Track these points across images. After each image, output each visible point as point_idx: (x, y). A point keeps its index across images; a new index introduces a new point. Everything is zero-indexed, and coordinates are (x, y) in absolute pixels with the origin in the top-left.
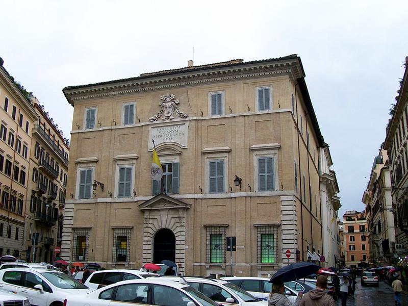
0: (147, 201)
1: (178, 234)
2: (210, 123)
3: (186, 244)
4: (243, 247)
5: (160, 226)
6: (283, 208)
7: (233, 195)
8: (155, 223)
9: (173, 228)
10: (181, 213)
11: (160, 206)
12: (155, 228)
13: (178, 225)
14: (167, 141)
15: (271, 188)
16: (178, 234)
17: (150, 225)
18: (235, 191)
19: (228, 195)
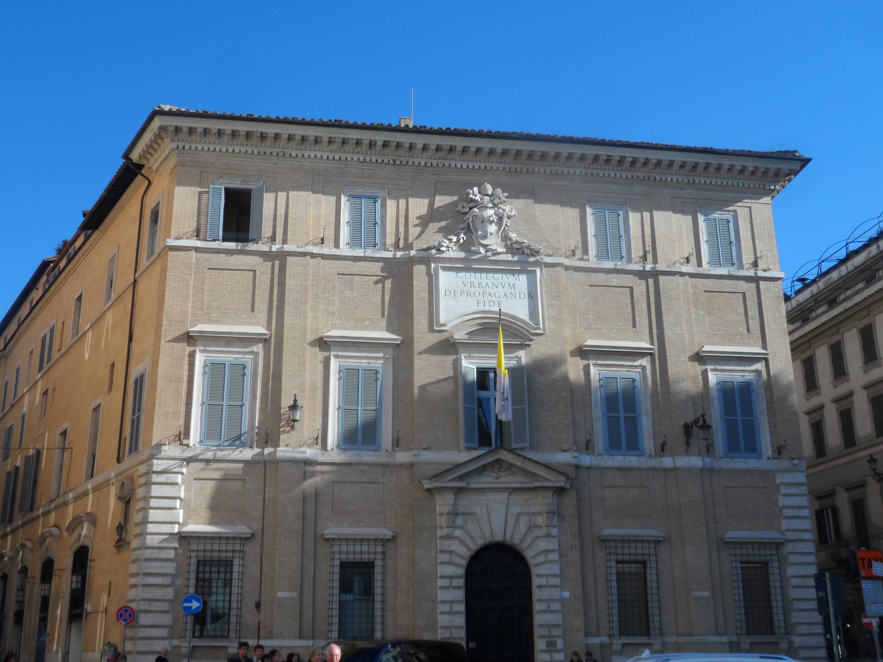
1: (541, 558)
2: (601, 278)
3: (562, 587)
4: (707, 594)
5: (488, 533)
7: (667, 462)
8: (471, 527)
9: (528, 542)
11: (483, 479)
12: (472, 538)
13: (540, 532)
14: (487, 308)
15: (752, 448)
16: (541, 558)
17: (457, 533)
18: (673, 454)
19: (653, 463)
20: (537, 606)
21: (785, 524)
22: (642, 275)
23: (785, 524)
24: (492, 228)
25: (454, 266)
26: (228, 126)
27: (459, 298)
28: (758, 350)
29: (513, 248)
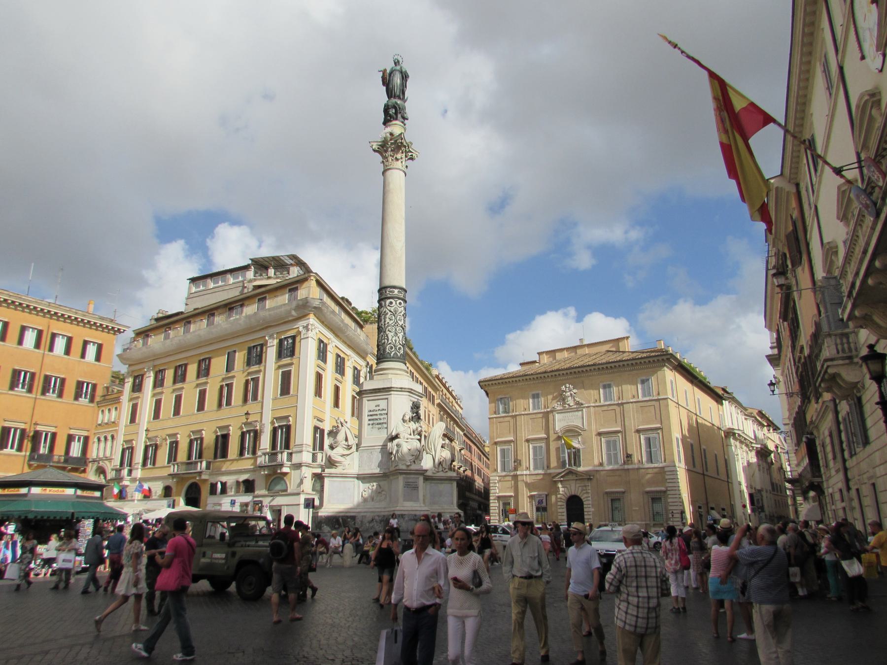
0: (560, 473)
2: (605, 408)
6: (667, 477)
7: (626, 467)
20: (565, 514)
21: (668, 485)
22: (618, 405)
24: (570, 398)
25: (560, 412)
26: (497, 382)
27: (560, 422)
28: (659, 425)
29: (578, 403)
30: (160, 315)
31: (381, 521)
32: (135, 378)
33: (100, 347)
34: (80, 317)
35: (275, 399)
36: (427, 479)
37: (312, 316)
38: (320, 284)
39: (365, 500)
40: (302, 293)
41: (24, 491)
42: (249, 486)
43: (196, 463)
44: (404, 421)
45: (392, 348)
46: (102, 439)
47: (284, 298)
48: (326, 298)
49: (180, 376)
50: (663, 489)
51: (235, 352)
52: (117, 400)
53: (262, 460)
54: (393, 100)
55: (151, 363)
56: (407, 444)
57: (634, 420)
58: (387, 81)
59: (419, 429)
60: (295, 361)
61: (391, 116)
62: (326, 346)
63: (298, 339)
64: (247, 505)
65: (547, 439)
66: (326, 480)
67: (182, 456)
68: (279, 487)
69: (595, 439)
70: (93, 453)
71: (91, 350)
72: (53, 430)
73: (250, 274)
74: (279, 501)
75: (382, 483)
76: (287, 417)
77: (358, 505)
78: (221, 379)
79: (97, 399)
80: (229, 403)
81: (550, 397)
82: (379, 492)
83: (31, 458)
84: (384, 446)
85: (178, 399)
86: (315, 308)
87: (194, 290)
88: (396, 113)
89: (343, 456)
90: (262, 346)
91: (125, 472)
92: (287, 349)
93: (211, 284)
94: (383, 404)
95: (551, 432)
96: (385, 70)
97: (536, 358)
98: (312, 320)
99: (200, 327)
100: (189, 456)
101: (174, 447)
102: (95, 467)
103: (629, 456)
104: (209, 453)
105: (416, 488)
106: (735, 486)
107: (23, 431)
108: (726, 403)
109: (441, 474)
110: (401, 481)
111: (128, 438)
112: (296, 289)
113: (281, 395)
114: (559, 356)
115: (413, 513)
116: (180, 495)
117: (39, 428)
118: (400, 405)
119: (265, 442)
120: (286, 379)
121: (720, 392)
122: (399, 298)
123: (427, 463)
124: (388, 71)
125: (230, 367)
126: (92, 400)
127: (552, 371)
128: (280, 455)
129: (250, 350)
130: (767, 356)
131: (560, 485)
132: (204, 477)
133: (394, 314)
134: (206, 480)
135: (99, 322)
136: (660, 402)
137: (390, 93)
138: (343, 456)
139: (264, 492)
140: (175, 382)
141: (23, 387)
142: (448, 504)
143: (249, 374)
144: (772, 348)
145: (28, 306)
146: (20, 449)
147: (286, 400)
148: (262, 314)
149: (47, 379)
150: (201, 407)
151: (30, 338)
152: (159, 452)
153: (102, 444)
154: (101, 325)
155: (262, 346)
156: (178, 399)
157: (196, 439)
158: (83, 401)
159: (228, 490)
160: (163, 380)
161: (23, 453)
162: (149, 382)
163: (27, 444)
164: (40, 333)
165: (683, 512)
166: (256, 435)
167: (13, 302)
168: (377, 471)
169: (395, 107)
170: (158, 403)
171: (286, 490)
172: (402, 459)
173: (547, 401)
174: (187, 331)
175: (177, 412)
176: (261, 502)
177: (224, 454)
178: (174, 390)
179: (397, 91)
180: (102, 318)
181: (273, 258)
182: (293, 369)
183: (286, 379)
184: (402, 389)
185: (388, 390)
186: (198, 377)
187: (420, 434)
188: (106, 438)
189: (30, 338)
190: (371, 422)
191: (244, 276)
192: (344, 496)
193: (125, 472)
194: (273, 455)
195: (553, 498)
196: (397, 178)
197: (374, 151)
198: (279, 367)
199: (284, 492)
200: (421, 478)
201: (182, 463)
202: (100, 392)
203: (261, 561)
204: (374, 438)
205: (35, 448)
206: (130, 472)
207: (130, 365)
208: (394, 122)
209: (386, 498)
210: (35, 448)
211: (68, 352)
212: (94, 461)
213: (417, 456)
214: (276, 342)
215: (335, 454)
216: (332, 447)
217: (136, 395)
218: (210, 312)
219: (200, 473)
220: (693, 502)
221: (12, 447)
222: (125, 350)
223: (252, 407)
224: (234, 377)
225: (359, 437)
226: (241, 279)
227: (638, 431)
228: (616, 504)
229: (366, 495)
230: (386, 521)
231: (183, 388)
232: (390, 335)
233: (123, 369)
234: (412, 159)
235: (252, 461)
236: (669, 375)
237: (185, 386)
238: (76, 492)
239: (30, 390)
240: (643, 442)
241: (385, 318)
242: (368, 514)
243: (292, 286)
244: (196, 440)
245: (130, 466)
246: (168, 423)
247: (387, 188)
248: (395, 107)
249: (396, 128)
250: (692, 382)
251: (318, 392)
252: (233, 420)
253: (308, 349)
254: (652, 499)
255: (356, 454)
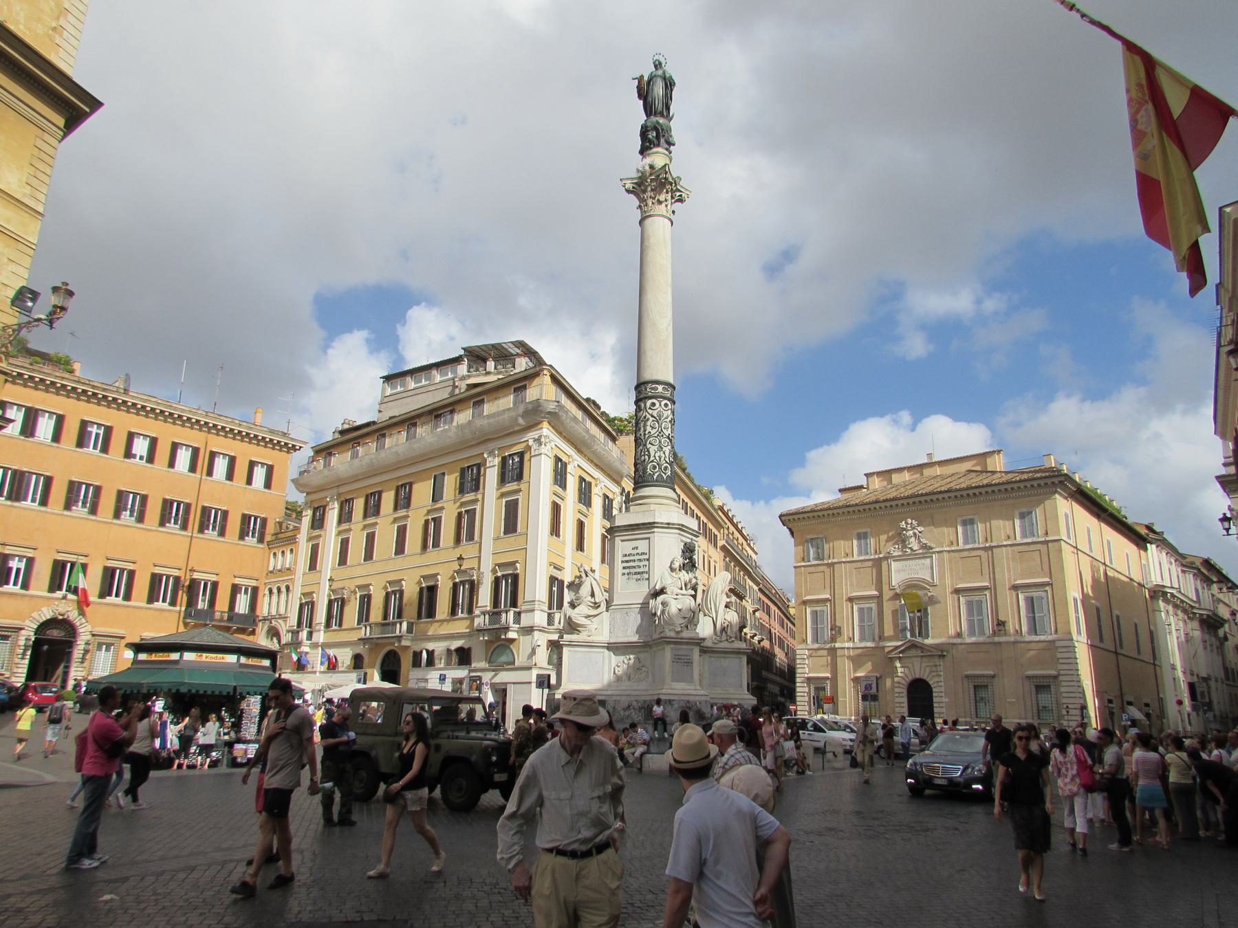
0: (897, 647)
2: (965, 554)
6: (1059, 656)
7: (997, 639)
10: (937, 661)
20: (906, 705)
21: (1061, 667)
22: (985, 549)
23: (1061, 667)
25: (897, 559)
27: (899, 573)
30: (346, 426)
31: (641, 708)
32: (315, 510)
33: (270, 470)
34: (245, 431)
35: (497, 539)
36: (705, 651)
37: (545, 424)
38: (557, 380)
39: (619, 679)
40: (532, 393)
41: (175, 656)
42: (463, 656)
43: (394, 624)
44: (672, 570)
45: (654, 467)
46: (275, 591)
47: (507, 401)
48: (565, 400)
49: (373, 508)
50: (1054, 672)
51: (443, 474)
52: (292, 540)
53: (479, 621)
54: (653, 119)
55: (335, 491)
56: (677, 602)
57: (1009, 571)
58: (644, 92)
59: (694, 581)
60: (523, 486)
61: (650, 142)
62: (565, 465)
63: (527, 457)
64: (461, 681)
65: (879, 598)
66: (565, 650)
67: (376, 615)
68: (503, 659)
69: (950, 600)
70: (263, 609)
71: (260, 474)
72: (214, 578)
73: (463, 369)
74: (503, 677)
75: (642, 656)
76: (513, 564)
77: (609, 685)
78: (425, 511)
79: (268, 538)
80: (436, 544)
81: (883, 537)
82: (637, 667)
83: (188, 615)
84: (645, 605)
85: (371, 538)
86: (549, 413)
87: (389, 391)
88: (658, 137)
89: (587, 617)
90: (479, 466)
91: (303, 635)
92: (514, 471)
93: (411, 384)
94: (642, 546)
95: (885, 588)
96: (642, 77)
97: (863, 481)
98: (546, 430)
99: (397, 442)
100: (386, 616)
101: (366, 601)
102: (266, 628)
103: (1001, 623)
104: (411, 611)
105: (689, 663)
106: (1166, 669)
107: (177, 579)
108: (1152, 548)
109: (725, 645)
110: (668, 653)
111: (307, 590)
112: (524, 387)
113: (505, 533)
114: (896, 478)
115: (686, 698)
116: (373, 667)
117: (196, 576)
118: (667, 548)
119: (484, 597)
120: (512, 511)
121: (1143, 531)
122: (665, 398)
123: (705, 629)
124: (646, 78)
125: (437, 496)
126: (261, 540)
127: (886, 500)
128: (504, 615)
129: (463, 472)
130: (1217, 478)
131: (898, 664)
132: (404, 643)
133: (658, 419)
134: (407, 647)
135: (268, 437)
136: (1049, 547)
137: (649, 110)
138: (587, 617)
139: (483, 664)
140: (365, 516)
141: (176, 523)
142: (737, 689)
143: (462, 504)
144: (1225, 465)
145: (180, 417)
146: (173, 603)
147: (512, 541)
148: (479, 423)
149: (206, 511)
150: (400, 549)
151: (184, 457)
152: (347, 609)
153: (275, 597)
154: (271, 440)
155: (479, 466)
156: (371, 538)
157: (394, 592)
158: (251, 540)
159: (437, 661)
160: (351, 512)
161: (178, 608)
162: (333, 515)
163: (183, 597)
164: (196, 452)
165: (1084, 707)
166: (473, 587)
167: (162, 412)
168: (635, 638)
169: (655, 128)
170: (345, 544)
171: (513, 663)
172: (669, 622)
173: (880, 544)
174: (381, 447)
175: (369, 556)
176: (480, 678)
177: (431, 613)
178: (365, 527)
179: (659, 106)
180: (272, 432)
181: (493, 345)
182: (520, 497)
183: (512, 511)
184: (669, 526)
185: (650, 526)
186: (396, 509)
187: (695, 588)
188: (279, 590)
189: (184, 457)
190: (627, 571)
191: (455, 372)
192: (591, 672)
193: (303, 635)
194: (495, 615)
195: (888, 682)
196: (659, 227)
197: (628, 191)
198: (503, 495)
199: (510, 665)
200: (696, 650)
201: (376, 624)
202: (270, 529)
203: (474, 758)
204: (631, 593)
205: (191, 602)
206: (310, 635)
207: (308, 494)
208: (655, 150)
209: (647, 676)
210: (191, 602)
211: (230, 476)
212: (265, 619)
213: (691, 619)
214: (497, 461)
215: (578, 615)
216: (573, 605)
217: (317, 532)
218: (409, 421)
219: (400, 638)
220: (1099, 693)
221: (164, 601)
222: (301, 473)
223: (467, 549)
224: (442, 508)
225: (610, 590)
226: (450, 376)
227: (1015, 588)
228: (982, 694)
229: (620, 671)
230: (647, 709)
231: (376, 524)
232: (652, 449)
233: (300, 498)
234: (681, 200)
235: (467, 623)
236: (1063, 506)
237: (378, 521)
238: (238, 659)
239: (184, 527)
240: (1022, 603)
241: (645, 426)
242: (623, 699)
243: (519, 384)
244: (394, 594)
245: (310, 626)
246: (358, 572)
247: (646, 243)
248: (655, 128)
249: (658, 158)
250: (1098, 516)
251: (555, 530)
252: (442, 566)
253: (541, 470)
254: (1037, 687)
255: (606, 615)
